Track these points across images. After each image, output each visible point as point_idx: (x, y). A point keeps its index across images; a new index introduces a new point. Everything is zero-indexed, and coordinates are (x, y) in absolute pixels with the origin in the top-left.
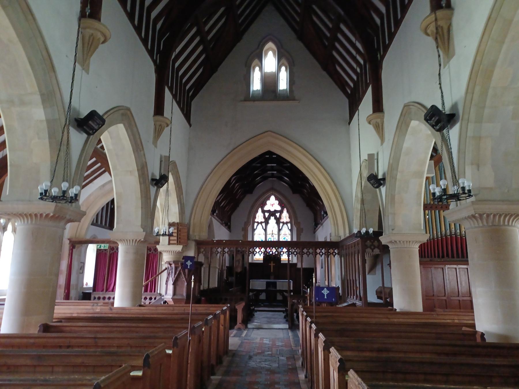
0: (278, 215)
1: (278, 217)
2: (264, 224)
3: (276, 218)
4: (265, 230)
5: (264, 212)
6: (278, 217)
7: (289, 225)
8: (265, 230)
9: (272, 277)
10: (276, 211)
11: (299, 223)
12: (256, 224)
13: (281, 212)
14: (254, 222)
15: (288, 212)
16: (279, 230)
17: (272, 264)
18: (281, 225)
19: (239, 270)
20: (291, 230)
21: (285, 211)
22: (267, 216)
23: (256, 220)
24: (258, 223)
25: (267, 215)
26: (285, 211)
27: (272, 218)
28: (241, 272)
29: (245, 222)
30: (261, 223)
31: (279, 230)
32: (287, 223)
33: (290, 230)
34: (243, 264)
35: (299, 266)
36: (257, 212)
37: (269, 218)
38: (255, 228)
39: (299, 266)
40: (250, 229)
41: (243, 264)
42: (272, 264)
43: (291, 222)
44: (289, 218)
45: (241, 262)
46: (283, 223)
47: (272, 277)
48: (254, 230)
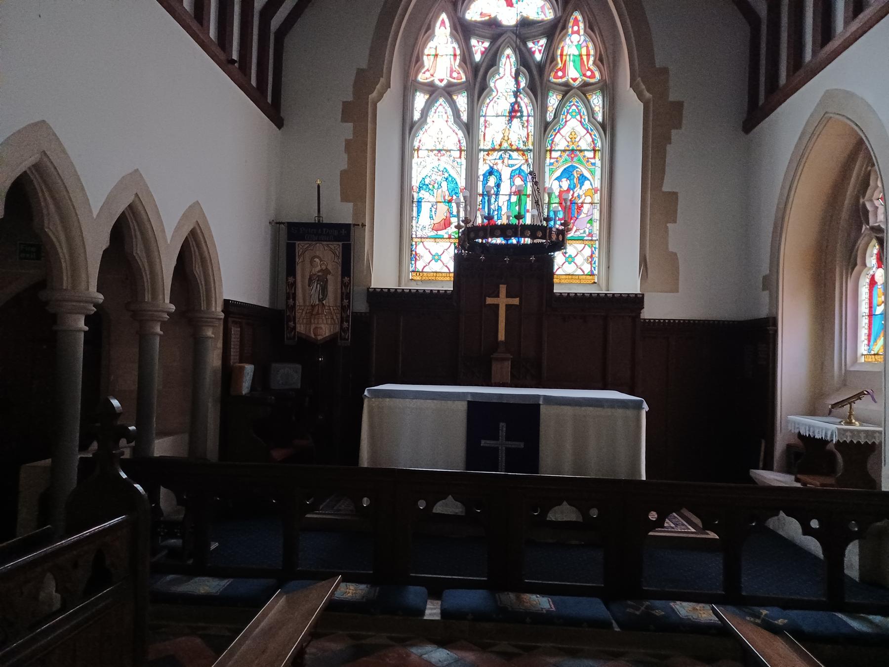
0: (537, 48)
1: (538, 57)
2: (462, 101)
3: (524, 60)
4: (470, 128)
5: (464, 31)
6: (538, 57)
7: (597, 101)
8: (470, 128)
9: (502, 368)
10: (526, 28)
11: (665, 71)
12: (420, 100)
13: (554, 31)
14: (409, 87)
15: (591, 27)
16: (545, 127)
17: (502, 301)
18: (553, 100)
19: (325, 329)
20: (608, 127)
21: (577, 23)
22: (478, 57)
23: (422, 78)
24: (432, 90)
25: (479, 47)
26: (577, 23)
27: (508, 62)
28: (332, 341)
29: (360, 72)
30: (449, 91)
31: (545, 127)
32: (585, 89)
33: (603, 125)
34: (346, 295)
35: (657, 308)
36: (429, 29)
37: (492, 60)
38: (417, 116)
39: (650, 312)
40: (386, 109)
41: (346, 295)
42: (502, 301)
43: (608, 89)
44: (600, 60)
45: (333, 286)
46: (566, 90)
47: (502, 368)
48: (409, 127)
